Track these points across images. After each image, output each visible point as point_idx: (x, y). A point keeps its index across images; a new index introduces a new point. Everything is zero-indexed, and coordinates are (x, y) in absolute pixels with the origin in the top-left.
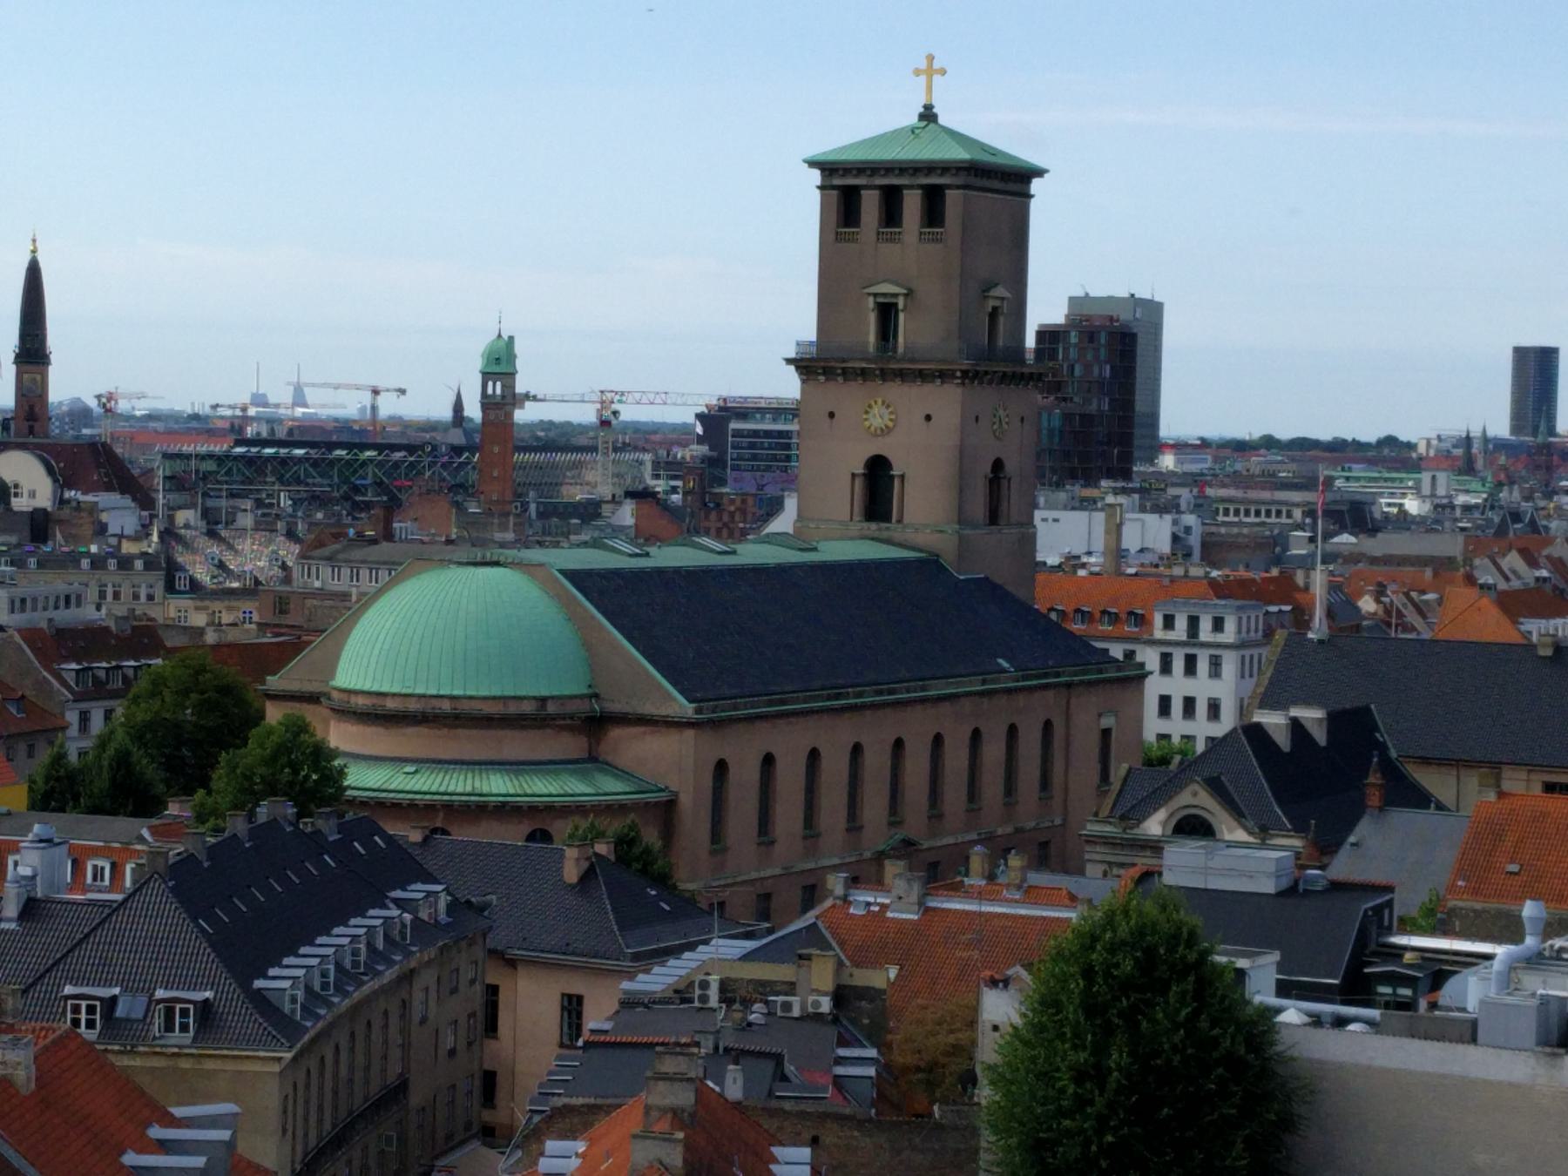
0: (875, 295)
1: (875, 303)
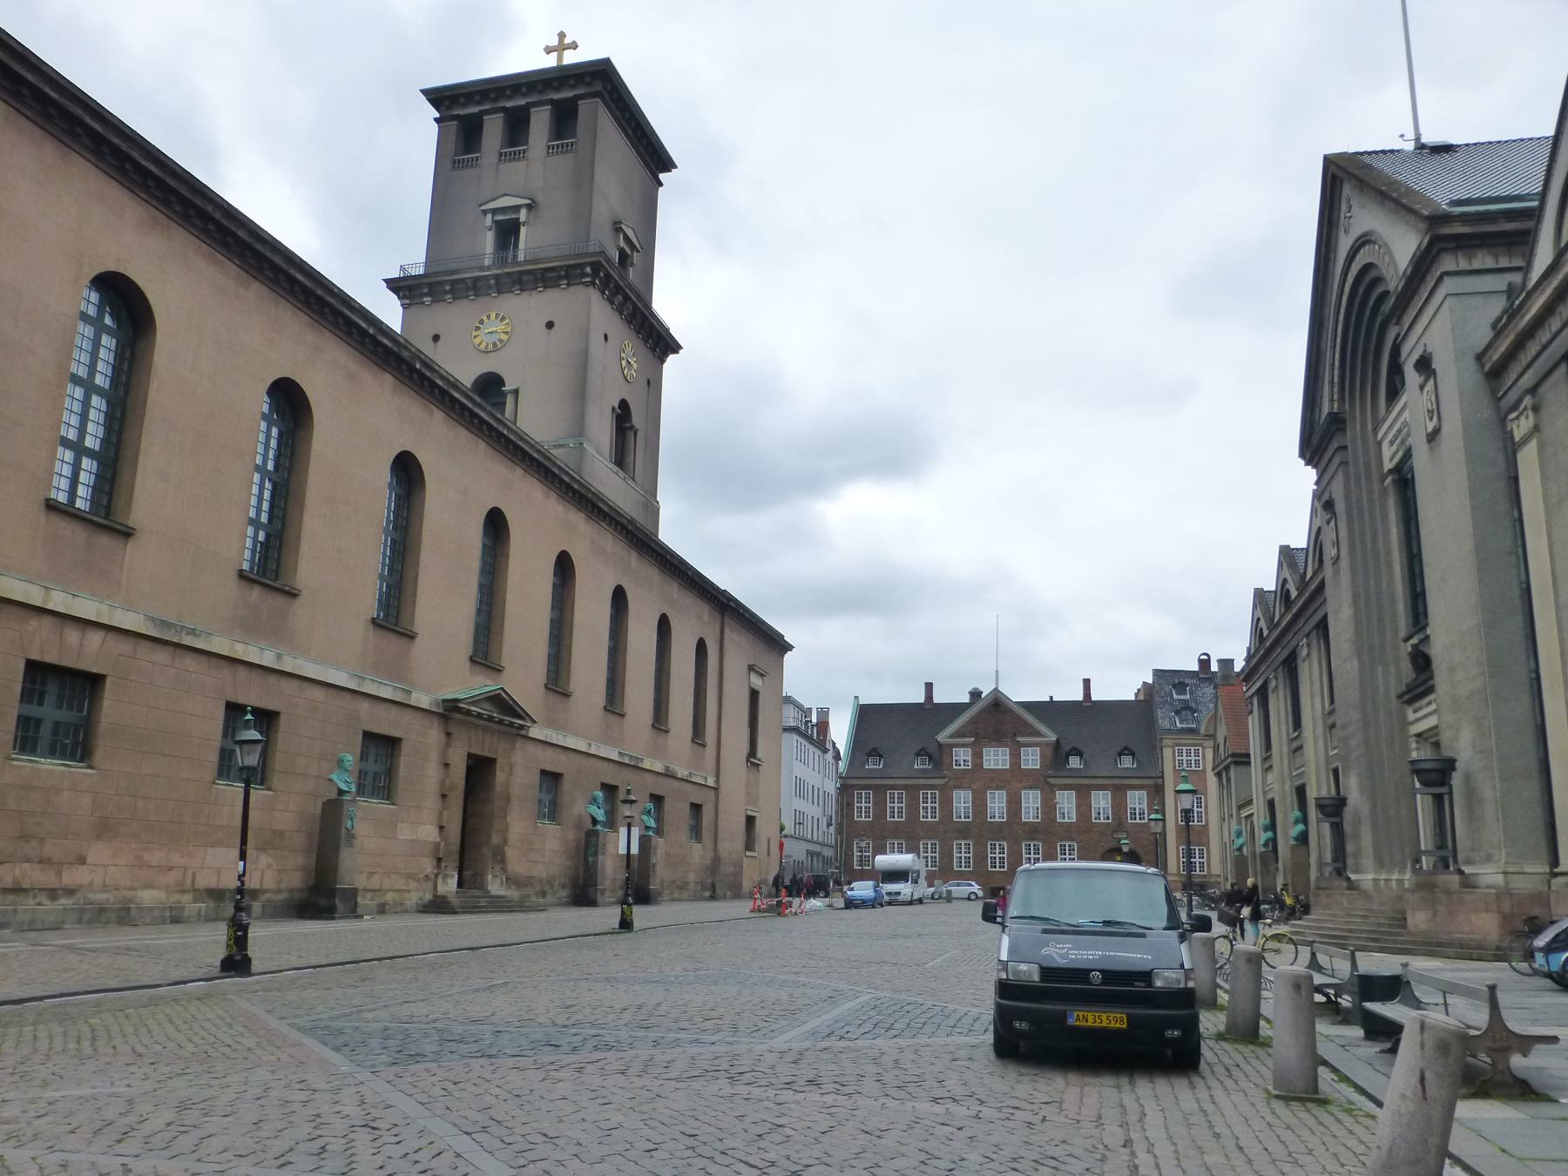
0: (495, 211)
1: (493, 221)
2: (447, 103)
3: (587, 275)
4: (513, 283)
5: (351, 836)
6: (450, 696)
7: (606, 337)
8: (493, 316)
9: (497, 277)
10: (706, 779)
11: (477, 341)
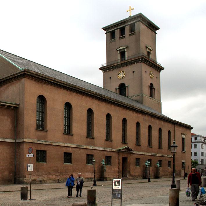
0: (119, 50)
1: (120, 52)
2: (107, 29)
3: (141, 60)
4: (125, 64)
5: (105, 170)
6: (119, 149)
7: (146, 72)
8: (121, 72)
9: (121, 64)
10: (171, 156)
11: (119, 77)
